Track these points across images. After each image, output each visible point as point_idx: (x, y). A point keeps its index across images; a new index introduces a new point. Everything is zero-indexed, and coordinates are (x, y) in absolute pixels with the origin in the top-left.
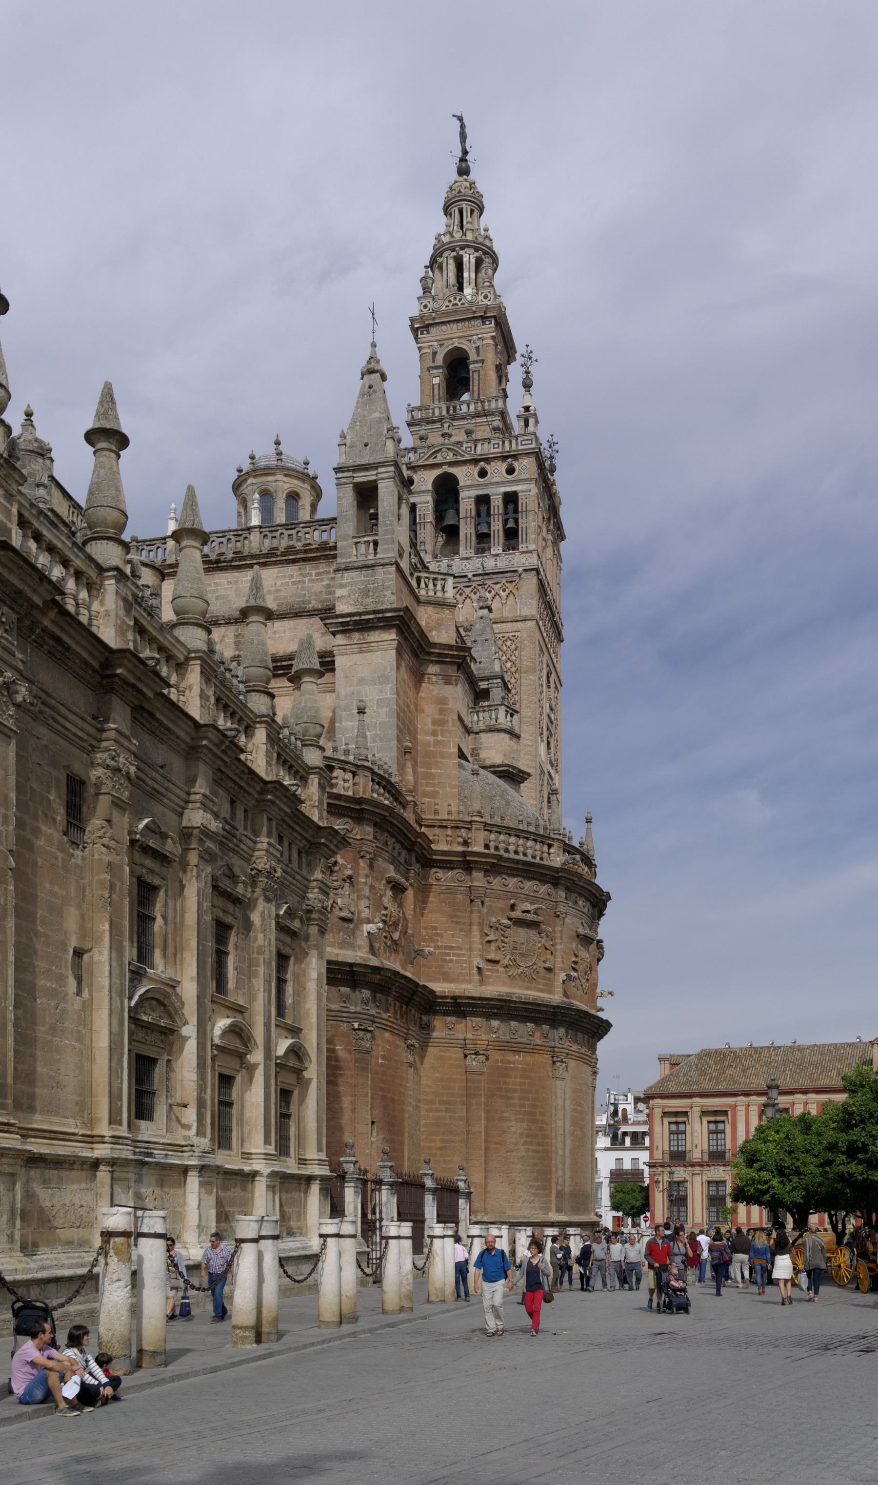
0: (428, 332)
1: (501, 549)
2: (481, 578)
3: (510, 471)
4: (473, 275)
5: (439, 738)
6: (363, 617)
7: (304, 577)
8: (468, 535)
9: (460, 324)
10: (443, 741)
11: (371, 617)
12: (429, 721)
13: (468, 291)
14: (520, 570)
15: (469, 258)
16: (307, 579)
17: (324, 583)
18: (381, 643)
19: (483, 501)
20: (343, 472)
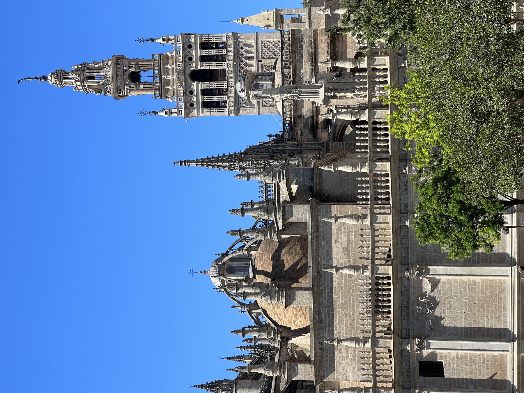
19: (203, 59)
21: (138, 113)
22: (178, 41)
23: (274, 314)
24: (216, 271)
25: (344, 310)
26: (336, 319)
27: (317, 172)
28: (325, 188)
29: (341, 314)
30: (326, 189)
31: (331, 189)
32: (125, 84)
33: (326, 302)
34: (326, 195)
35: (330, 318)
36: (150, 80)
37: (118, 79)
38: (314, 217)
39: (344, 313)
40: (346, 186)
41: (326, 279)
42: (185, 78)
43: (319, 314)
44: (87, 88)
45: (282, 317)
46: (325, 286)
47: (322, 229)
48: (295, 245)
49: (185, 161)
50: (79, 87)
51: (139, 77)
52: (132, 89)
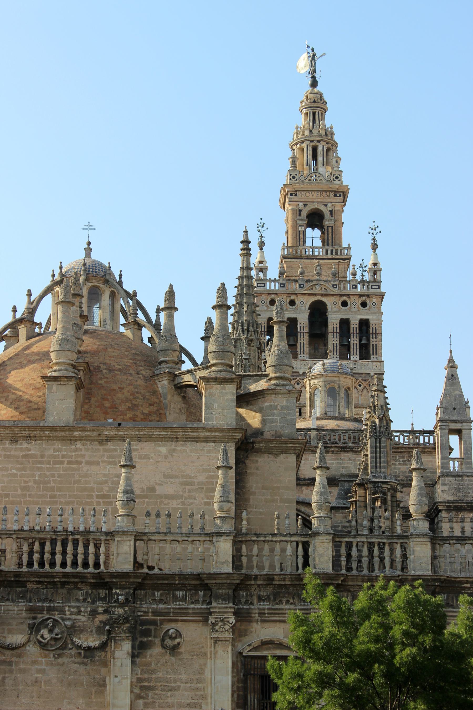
0: (296, 195)
1: (358, 357)
3: (364, 304)
7: (396, 462)
8: (335, 345)
9: (319, 193)
11: (464, 505)
14: (372, 374)
16: (397, 463)
19: (345, 323)
21: (261, 219)
22: (373, 287)
23: (20, 362)
24: (94, 268)
25: (36, 486)
26: (18, 469)
27: (290, 445)
28: (260, 460)
29: (27, 480)
30: (257, 461)
31: (257, 469)
32: (305, 203)
33: (51, 452)
34: (247, 462)
35: (20, 459)
36: (308, 243)
37: (313, 193)
38: (213, 434)
39: (30, 484)
40: (263, 498)
41: (95, 454)
42: (316, 295)
43: (30, 437)
45: (15, 377)
46: (83, 450)
47: (191, 448)
48: (150, 405)
49: (250, 250)
50: (301, 133)
51: (313, 228)
52: (298, 213)
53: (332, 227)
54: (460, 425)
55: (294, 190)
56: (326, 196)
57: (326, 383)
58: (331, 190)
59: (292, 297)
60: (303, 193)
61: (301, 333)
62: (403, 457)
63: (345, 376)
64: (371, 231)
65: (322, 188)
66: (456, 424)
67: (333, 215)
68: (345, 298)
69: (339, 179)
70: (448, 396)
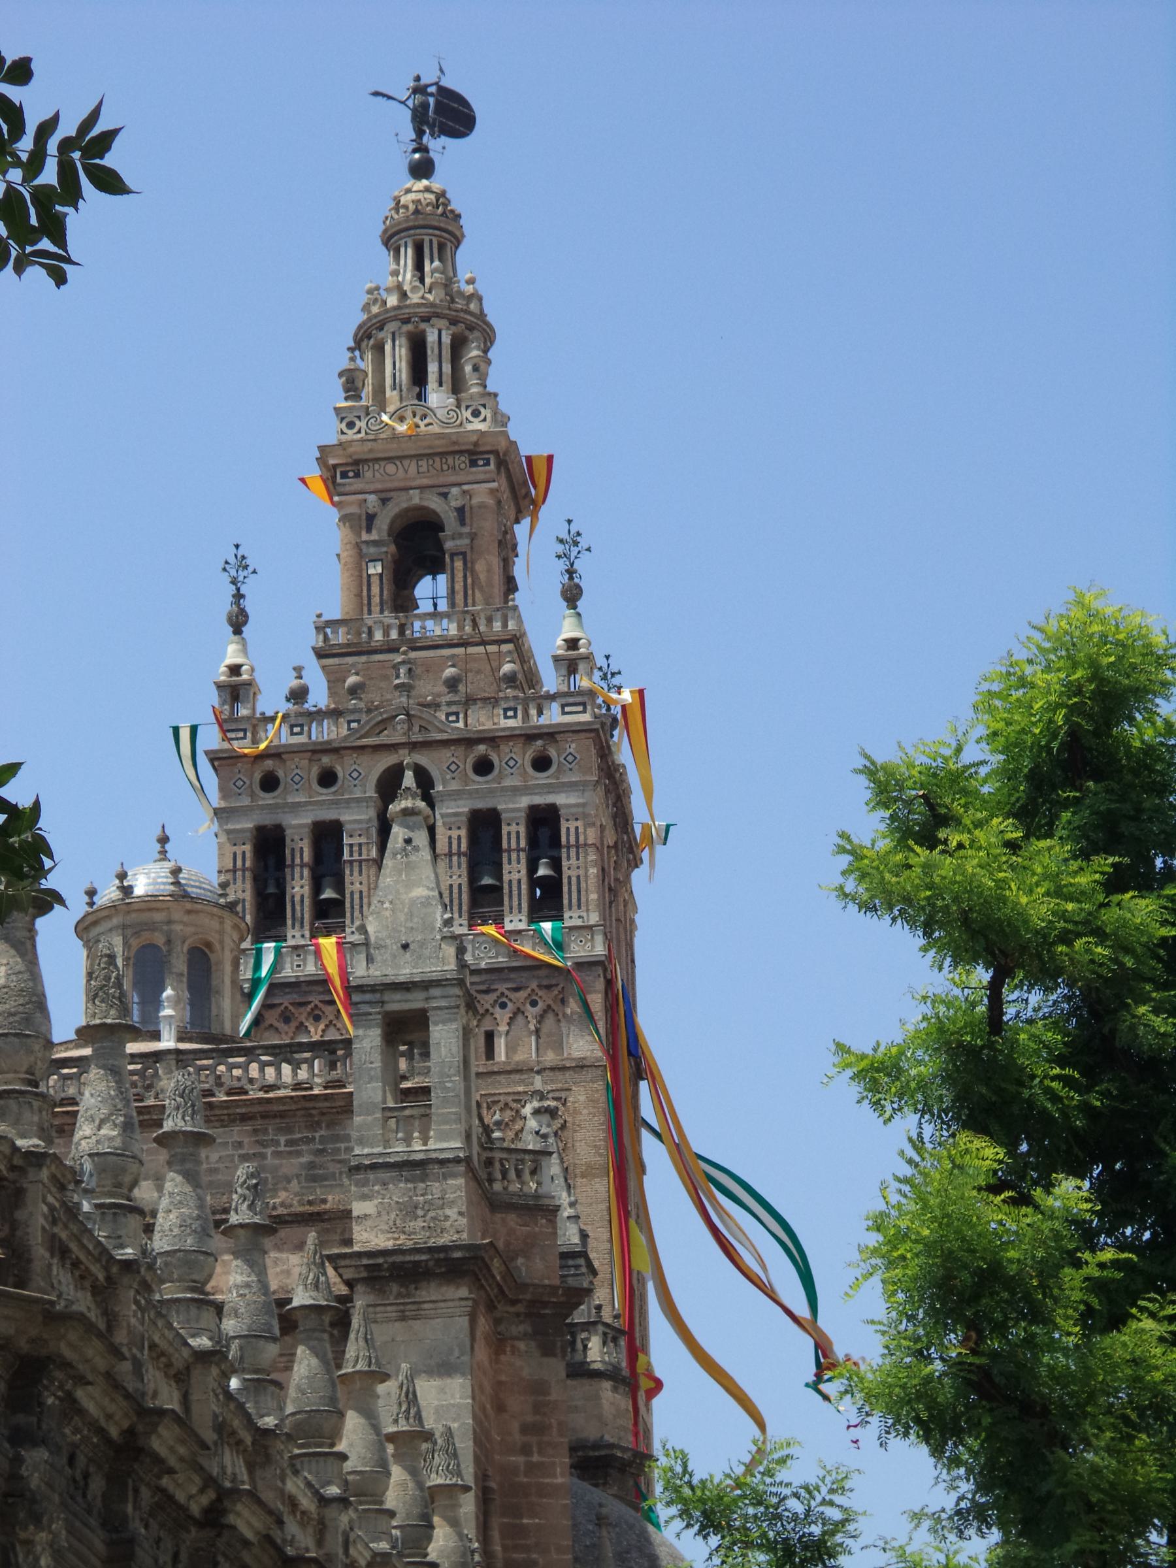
0: (357, 475)
1: (524, 918)
2: (484, 977)
4: (447, 368)
5: (535, 1458)
6: (408, 1258)
7: (265, 1147)
8: (455, 890)
9: (423, 463)
10: (542, 1463)
11: (424, 1257)
12: (515, 1426)
13: (437, 397)
15: (436, 336)
17: (304, 1160)
18: (442, 1305)
20: (364, 992)
32: (383, 495)
37: (406, 462)
44: (372, 342)
52: (364, 524)
53: (464, 554)
54: (421, 995)
55: (350, 460)
56: (445, 467)
57: (129, 932)
58: (456, 448)
59: (326, 760)
60: (377, 466)
61: (351, 862)
62: (288, 1130)
63: (189, 906)
64: (560, 548)
65: (430, 447)
66: (409, 996)
67: (468, 521)
68: (482, 748)
69: (482, 417)
70: (387, 905)
